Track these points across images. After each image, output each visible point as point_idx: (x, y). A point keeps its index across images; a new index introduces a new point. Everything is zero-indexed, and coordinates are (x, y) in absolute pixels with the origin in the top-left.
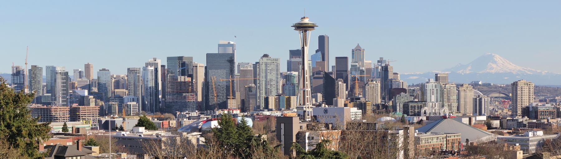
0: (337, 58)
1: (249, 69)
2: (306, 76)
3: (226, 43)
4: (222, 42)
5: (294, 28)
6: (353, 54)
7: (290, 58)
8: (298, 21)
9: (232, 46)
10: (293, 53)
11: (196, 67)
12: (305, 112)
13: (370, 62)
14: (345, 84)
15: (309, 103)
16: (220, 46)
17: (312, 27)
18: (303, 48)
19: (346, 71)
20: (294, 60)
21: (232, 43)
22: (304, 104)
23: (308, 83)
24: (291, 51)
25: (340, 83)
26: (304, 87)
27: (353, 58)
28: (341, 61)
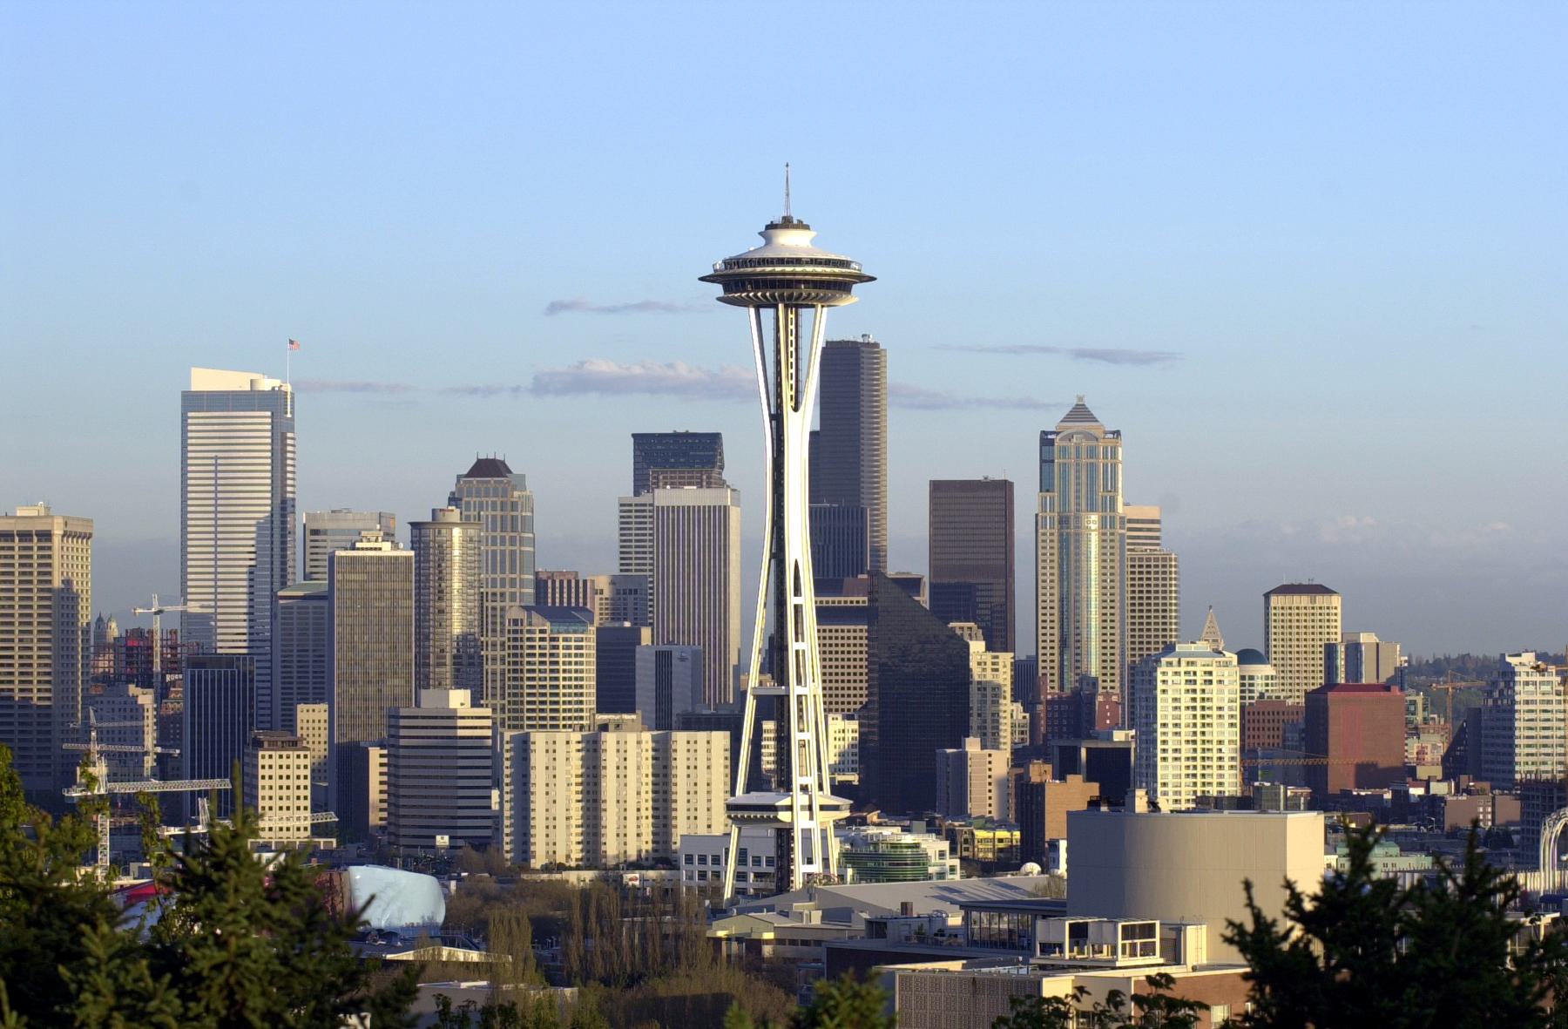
0: (937, 487)
1: (387, 549)
2: (792, 601)
3: (234, 381)
4: (205, 380)
5: (718, 289)
6: (1046, 462)
7: (642, 483)
8: (747, 243)
9: (273, 402)
10: (677, 455)
11: (46, 536)
12: (784, 835)
13: (1152, 512)
14: (1006, 659)
15: (812, 781)
16: (194, 401)
17: (835, 283)
18: (777, 419)
19: (1007, 571)
20: (666, 496)
21: (266, 384)
22: (786, 785)
23: (806, 645)
24: (639, 438)
25: (977, 647)
26: (782, 679)
27: (1045, 485)
28: (971, 509)
